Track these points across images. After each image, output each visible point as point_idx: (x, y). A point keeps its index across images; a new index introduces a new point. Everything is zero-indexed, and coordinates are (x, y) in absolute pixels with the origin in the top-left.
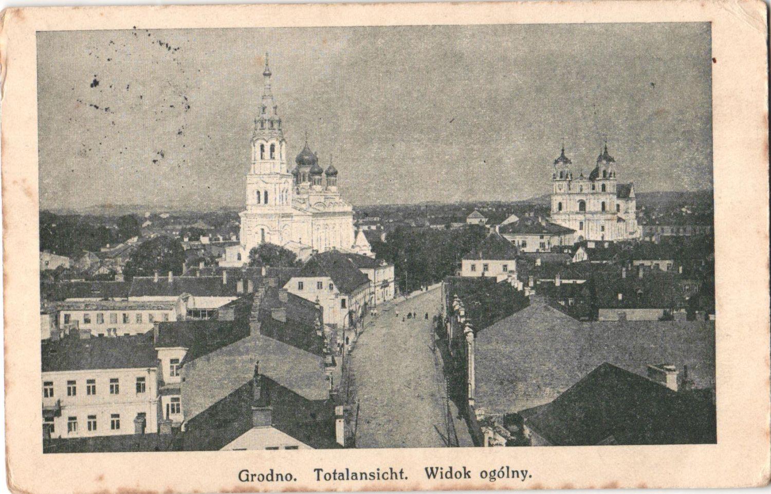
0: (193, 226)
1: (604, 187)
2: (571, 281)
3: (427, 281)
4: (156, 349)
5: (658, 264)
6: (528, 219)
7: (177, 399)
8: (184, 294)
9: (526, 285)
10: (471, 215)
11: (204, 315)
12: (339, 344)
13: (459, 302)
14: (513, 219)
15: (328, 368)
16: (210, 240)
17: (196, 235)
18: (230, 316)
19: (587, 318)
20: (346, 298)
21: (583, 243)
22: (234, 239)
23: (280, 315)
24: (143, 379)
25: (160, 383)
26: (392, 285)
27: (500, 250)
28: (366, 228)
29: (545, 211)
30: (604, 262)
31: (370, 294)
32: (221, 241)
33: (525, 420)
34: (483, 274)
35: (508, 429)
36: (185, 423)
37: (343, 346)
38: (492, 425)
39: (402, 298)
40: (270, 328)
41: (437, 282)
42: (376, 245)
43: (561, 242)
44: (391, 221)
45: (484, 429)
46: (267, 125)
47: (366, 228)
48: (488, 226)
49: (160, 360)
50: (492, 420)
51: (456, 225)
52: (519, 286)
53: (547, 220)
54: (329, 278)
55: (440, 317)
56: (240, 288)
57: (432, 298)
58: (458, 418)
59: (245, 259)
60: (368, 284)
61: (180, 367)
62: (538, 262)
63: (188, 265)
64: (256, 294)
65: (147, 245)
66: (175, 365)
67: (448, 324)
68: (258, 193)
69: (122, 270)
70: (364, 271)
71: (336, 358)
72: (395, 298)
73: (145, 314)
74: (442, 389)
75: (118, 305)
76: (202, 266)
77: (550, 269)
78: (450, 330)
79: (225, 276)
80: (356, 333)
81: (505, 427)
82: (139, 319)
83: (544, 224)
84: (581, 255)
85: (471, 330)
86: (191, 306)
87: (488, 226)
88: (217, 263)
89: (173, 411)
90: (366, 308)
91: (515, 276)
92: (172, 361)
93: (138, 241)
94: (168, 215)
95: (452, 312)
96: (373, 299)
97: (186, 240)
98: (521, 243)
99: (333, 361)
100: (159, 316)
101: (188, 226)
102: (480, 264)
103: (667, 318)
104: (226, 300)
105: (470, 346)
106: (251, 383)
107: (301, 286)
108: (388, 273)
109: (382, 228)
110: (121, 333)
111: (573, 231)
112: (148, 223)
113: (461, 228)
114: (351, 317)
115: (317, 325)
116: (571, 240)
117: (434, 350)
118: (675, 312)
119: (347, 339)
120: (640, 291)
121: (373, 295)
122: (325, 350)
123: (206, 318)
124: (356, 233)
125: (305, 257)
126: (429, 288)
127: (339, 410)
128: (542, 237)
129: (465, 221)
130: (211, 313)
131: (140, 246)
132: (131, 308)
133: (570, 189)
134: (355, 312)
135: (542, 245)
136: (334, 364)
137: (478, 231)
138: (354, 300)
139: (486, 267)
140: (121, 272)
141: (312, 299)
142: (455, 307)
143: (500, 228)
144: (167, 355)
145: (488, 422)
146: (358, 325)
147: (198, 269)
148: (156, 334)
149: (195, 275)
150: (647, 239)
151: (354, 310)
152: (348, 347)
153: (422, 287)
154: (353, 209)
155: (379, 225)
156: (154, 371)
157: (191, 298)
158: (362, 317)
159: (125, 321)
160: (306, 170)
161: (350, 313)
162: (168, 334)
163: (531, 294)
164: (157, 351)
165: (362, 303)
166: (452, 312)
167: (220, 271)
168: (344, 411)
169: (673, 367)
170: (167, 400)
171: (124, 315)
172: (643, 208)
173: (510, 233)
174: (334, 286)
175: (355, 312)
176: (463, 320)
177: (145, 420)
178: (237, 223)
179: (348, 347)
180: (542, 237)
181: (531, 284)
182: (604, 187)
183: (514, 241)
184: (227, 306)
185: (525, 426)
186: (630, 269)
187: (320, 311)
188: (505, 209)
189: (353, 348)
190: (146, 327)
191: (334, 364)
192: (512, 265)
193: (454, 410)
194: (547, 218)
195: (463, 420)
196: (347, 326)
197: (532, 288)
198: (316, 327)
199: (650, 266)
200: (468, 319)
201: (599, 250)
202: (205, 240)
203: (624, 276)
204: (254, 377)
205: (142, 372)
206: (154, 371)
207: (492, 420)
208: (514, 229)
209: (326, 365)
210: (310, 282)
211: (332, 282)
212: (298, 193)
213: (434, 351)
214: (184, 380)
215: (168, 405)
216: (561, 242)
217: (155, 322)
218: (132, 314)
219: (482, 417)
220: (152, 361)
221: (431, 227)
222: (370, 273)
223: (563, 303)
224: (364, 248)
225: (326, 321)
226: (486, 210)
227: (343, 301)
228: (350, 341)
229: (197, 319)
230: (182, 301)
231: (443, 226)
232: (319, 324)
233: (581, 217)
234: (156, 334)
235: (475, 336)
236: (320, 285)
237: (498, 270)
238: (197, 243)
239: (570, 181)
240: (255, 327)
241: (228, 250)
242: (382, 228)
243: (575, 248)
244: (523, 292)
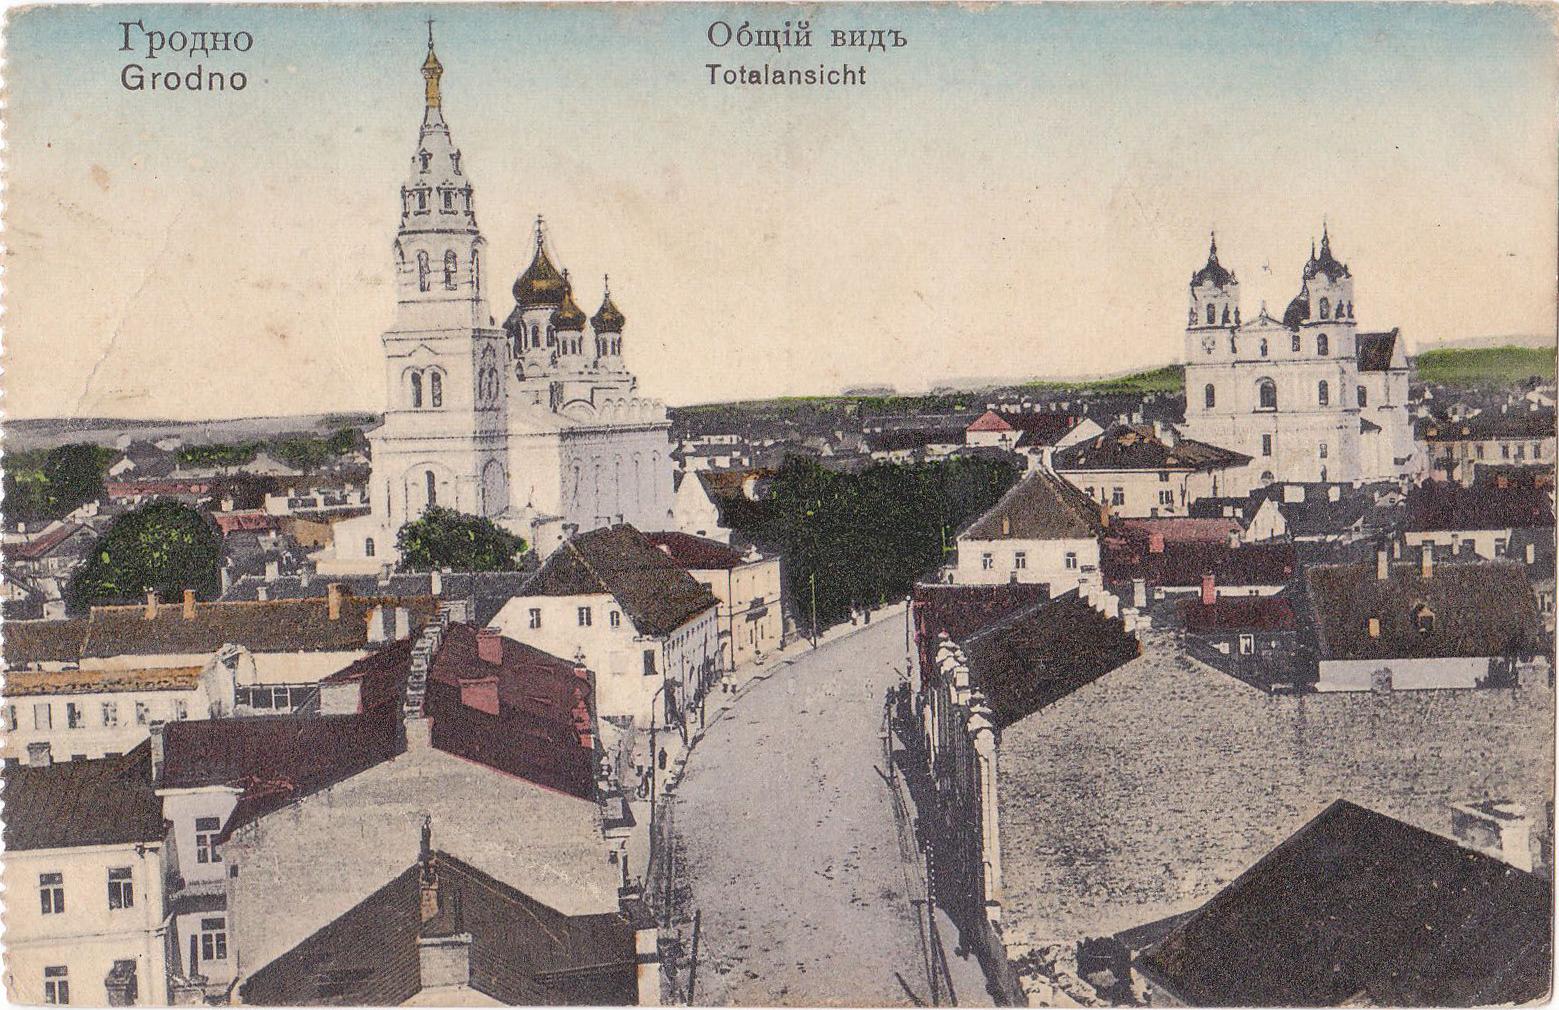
0: (244, 468)
1: (1323, 340)
2: (1243, 591)
3: (870, 601)
4: (158, 793)
5: (1472, 542)
6: (1123, 431)
7: (220, 923)
8: (226, 647)
9: (1127, 600)
10: (977, 424)
11: (281, 702)
12: (640, 769)
13: (953, 650)
14: (1087, 430)
15: (613, 832)
16: (292, 504)
17: (254, 491)
18: (344, 701)
19: (1290, 686)
20: (656, 646)
22: (354, 501)
23: (481, 697)
24: (126, 872)
25: (173, 879)
26: (775, 611)
27: (1055, 512)
28: (702, 463)
29: (1173, 409)
30: (1330, 538)
31: (720, 635)
32: (321, 507)
33: (1134, 954)
34: (1014, 580)
35: (1089, 982)
36: (237, 985)
37: (651, 773)
38: (1047, 970)
39: (804, 645)
40: (458, 734)
41: (891, 601)
42: (732, 510)
43: (1215, 488)
44: (769, 443)
45: (1026, 981)
46: (435, 202)
47: (702, 463)
48: (1024, 451)
50: (1049, 958)
51: (939, 451)
52: (1107, 604)
53: (1176, 433)
54: (611, 597)
55: (906, 689)
56: (376, 631)
57: (880, 642)
58: (958, 953)
59: (389, 553)
60: (711, 612)
61: (225, 837)
62: (1157, 546)
63: (234, 574)
64: (419, 644)
65: (129, 522)
66: (208, 833)
67: (927, 710)
68: (416, 379)
69: (61, 590)
70: (700, 576)
71: (633, 806)
72: (783, 645)
74: (917, 873)
75: (51, 681)
76: (272, 572)
77: (1185, 560)
78: (931, 725)
79: (334, 598)
80: (685, 740)
81: (1083, 973)
82: (109, 717)
83: (1168, 441)
84: (1268, 523)
85: (987, 724)
86: (246, 679)
87: (1024, 451)
88: (312, 566)
89: (208, 955)
90: (709, 674)
91: (1096, 578)
92: (203, 823)
93: (100, 512)
94: (177, 443)
95: (932, 675)
96: (727, 649)
97: (227, 505)
98: (1110, 497)
99: (626, 810)
100: (163, 707)
101: (233, 471)
102: (1004, 550)
103: (1498, 680)
104: (343, 660)
105: (984, 765)
106: (412, 873)
108: (760, 579)
109: (746, 462)
110: (62, 755)
111: (1244, 460)
112: (126, 464)
113: (953, 457)
114: (670, 698)
115: (580, 720)
116: (1237, 483)
117: (892, 777)
118: (1519, 664)
119: (663, 755)
120: (1426, 612)
121: (727, 639)
122: (603, 786)
123: (287, 710)
124: (678, 478)
125: (548, 543)
126: (874, 615)
127: (647, 941)
128: (1164, 477)
129: (959, 436)
130: (304, 695)
131: (104, 526)
132: (87, 688)
133: (1234, 350)
134: (680, 685)
135: (1166, 497)
136: (628, 821)
137: (1000, 469)
138: (676, 654)
139: (1021, 559)
140: (58, 595)
141: (566, 654)
142: (941, 663)
143: (1053, 455)
144: (182, 805)
145: (1037, 963)
146: (690, 717)
147: (263, 583)
148: (158, 755)
149: (254, 596)
150: (1441, 476)
151: (678, 679)
152: (664, 777)
153: (854, 614)
154: (668, 416)
155: (736, 454)
156: (154, 850)
157: (244, 661)
158: (700, 695)
159: (72, 724)
160: (542, 316)
161: (669, 687)
162: (193, 750)
163: (1140, 626)
164: (161, 798)
165: (699, 661)
166: (932, 675)
167: (321, 584)
168: (659, 941)
169: (1516, 809)
170: (190, 925)
171: (71, 706)
172: (1428, 395)
173: (1087, 466)
174: (624, 618)
175: (680, 685)
176: (964, 698)
177: (134, 978)
178: (362, 460)
179: (664, 777)
180: (1164, 477)
181: (1140, 599)
182: (1323, 340)
183: (1091, 489)
184: (339, 678)
185: (1133, 971)
186: (1397, 555)
187: (588, 682)
188: (1065, 406)
189: (680, 777)
190: (127, 738)
191: (628, 821)
192: (1088, 551)
193: (951, 935)
194: (1178, 427)
195: (972, 957)
196: (660, 722)
197: (1143, 612)
198: (580, 726)
199: (1450, 547)
200: (978, 695)
201: (1313, 509)
202: (276, 506)
203: (1383, 572)
204: (421, 858)
206: (151, 850)
207: (1049, 958)
208: (1098, 456)
209: (609, 824)
210: (560, 610)
211: (617, 607)
212: (522, 378)
213: (891, 782)
214: (234, 871)
215: (194, 938)
216: (1215, 488)
217: (154, 723)
218: (90, 705)
219: (1024, 951)
220: (153, 827)
221: (875, 456)
222: (716, 579)
223: (1224, 648)
224: (698, 516)
225: (600, 713)
226: (1015, 409)
227: (649, 658)
228: (670, 763)
229: (261, 712)
230: (222, 667)
231: (908, 452)
232: (586, 716)
233: (1266, 423)
234: (158, 755)
235: (997, 743)
236: (585, 617)
237: (1058, 564)
238: (254, 513)
239: (1233, 330)
240: (418, 729)
241: (339, 527)
242: (746, 462)
243: (1250, 506)
244: (1119, 623)
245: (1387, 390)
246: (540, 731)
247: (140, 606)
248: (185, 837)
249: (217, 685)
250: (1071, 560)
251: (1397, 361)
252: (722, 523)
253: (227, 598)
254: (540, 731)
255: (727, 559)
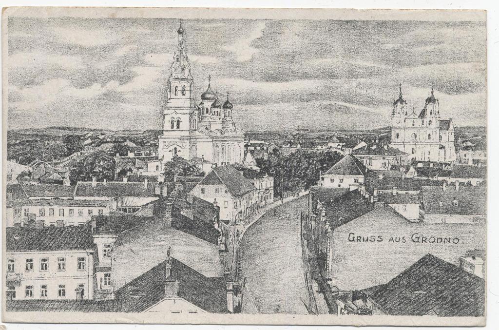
14: (363, 144)
20: (238, 201)
21: (414, 163)
29: (388, 139)
42: (259, 162)
49: (96, 244)
73: (85, 210)
82: (81, 213)
100: (95, 212)
102: (337, 178)
107: (203, 190)
108: (268, 182)
112: (89, 141)
125: (207, 169)
135: (384, 164)
141: (211, 201)
170: (100, 275)
180: (384, 158)
181: (375, 194)
190: (85, 219)
192: (361, 179)
193: (316, 287)
205: (81, 253)
210: (210, 189)
234: (94, 225)
236: (217, 191)
245: (448, 137)
246: (203, 225)
247: (90, 182)
248: (101, 249)
249: (110, 207)
250: (356, 181)
251: (451, 127)
252: (257, 166)
253: (116, 181)
254: (203, 225)
255: (259, 175)
